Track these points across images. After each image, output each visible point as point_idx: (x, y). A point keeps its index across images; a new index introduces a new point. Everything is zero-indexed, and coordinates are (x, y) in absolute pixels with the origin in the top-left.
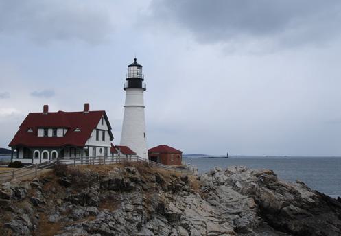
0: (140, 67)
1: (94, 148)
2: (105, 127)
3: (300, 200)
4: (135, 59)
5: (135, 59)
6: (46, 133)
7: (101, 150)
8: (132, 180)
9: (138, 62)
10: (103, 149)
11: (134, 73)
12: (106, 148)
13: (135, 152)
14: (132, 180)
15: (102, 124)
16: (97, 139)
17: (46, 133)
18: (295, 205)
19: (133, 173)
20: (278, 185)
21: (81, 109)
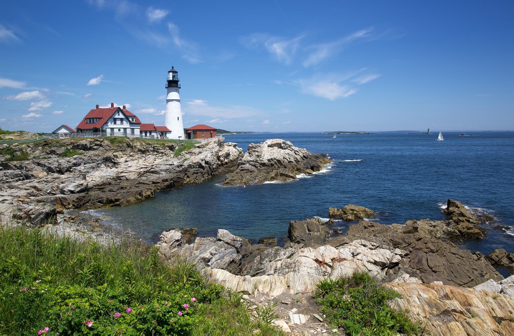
0: (175, 72)
1: (112, 129)
2: (121, 116)
3: (257, 161)
4: (173, 67)
5: (173, 67)
6: (90, 121)
7: (119, 130)
8: (96, 145)
9: (175, 69)
10: (122, 130)
11: (171, 77)
12: (125, 129)
13: (171, 130)
14: (96, 145)
15: (119, 115)
16: (115, 123)
17: (90, 121)
18: (251, 165)
19: (102, 142)
20: (254, 151)
21: (109, 106)
